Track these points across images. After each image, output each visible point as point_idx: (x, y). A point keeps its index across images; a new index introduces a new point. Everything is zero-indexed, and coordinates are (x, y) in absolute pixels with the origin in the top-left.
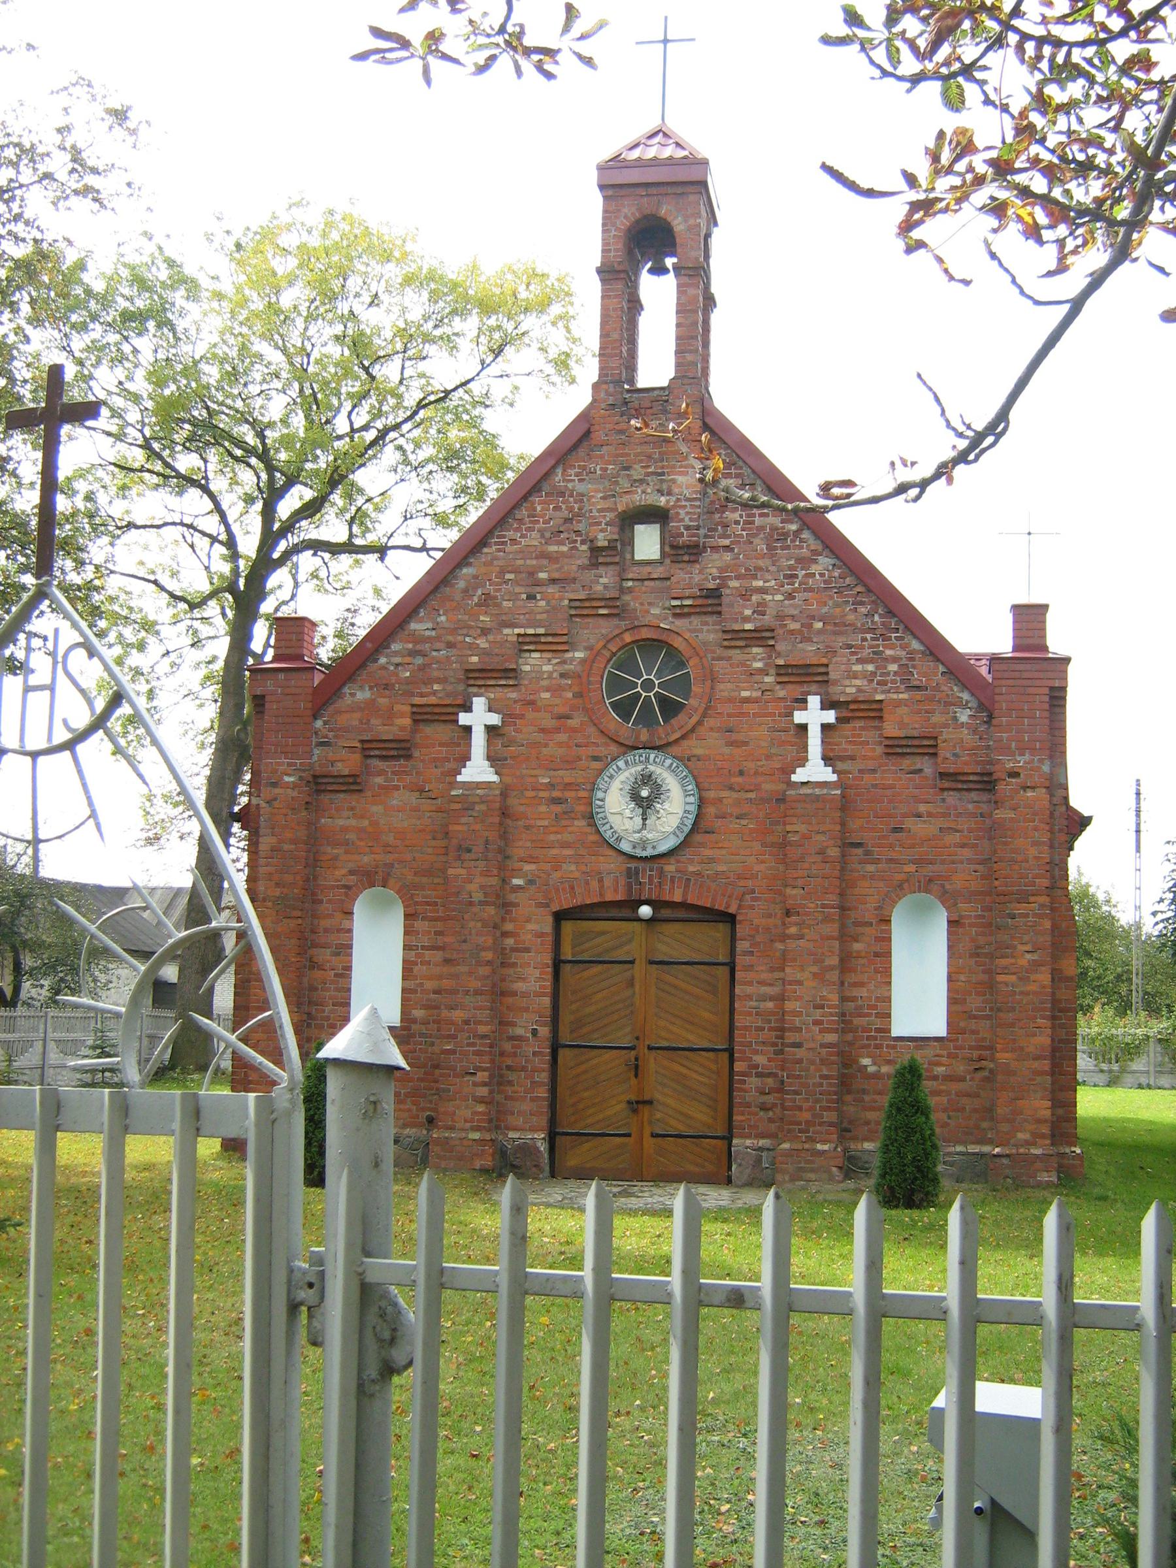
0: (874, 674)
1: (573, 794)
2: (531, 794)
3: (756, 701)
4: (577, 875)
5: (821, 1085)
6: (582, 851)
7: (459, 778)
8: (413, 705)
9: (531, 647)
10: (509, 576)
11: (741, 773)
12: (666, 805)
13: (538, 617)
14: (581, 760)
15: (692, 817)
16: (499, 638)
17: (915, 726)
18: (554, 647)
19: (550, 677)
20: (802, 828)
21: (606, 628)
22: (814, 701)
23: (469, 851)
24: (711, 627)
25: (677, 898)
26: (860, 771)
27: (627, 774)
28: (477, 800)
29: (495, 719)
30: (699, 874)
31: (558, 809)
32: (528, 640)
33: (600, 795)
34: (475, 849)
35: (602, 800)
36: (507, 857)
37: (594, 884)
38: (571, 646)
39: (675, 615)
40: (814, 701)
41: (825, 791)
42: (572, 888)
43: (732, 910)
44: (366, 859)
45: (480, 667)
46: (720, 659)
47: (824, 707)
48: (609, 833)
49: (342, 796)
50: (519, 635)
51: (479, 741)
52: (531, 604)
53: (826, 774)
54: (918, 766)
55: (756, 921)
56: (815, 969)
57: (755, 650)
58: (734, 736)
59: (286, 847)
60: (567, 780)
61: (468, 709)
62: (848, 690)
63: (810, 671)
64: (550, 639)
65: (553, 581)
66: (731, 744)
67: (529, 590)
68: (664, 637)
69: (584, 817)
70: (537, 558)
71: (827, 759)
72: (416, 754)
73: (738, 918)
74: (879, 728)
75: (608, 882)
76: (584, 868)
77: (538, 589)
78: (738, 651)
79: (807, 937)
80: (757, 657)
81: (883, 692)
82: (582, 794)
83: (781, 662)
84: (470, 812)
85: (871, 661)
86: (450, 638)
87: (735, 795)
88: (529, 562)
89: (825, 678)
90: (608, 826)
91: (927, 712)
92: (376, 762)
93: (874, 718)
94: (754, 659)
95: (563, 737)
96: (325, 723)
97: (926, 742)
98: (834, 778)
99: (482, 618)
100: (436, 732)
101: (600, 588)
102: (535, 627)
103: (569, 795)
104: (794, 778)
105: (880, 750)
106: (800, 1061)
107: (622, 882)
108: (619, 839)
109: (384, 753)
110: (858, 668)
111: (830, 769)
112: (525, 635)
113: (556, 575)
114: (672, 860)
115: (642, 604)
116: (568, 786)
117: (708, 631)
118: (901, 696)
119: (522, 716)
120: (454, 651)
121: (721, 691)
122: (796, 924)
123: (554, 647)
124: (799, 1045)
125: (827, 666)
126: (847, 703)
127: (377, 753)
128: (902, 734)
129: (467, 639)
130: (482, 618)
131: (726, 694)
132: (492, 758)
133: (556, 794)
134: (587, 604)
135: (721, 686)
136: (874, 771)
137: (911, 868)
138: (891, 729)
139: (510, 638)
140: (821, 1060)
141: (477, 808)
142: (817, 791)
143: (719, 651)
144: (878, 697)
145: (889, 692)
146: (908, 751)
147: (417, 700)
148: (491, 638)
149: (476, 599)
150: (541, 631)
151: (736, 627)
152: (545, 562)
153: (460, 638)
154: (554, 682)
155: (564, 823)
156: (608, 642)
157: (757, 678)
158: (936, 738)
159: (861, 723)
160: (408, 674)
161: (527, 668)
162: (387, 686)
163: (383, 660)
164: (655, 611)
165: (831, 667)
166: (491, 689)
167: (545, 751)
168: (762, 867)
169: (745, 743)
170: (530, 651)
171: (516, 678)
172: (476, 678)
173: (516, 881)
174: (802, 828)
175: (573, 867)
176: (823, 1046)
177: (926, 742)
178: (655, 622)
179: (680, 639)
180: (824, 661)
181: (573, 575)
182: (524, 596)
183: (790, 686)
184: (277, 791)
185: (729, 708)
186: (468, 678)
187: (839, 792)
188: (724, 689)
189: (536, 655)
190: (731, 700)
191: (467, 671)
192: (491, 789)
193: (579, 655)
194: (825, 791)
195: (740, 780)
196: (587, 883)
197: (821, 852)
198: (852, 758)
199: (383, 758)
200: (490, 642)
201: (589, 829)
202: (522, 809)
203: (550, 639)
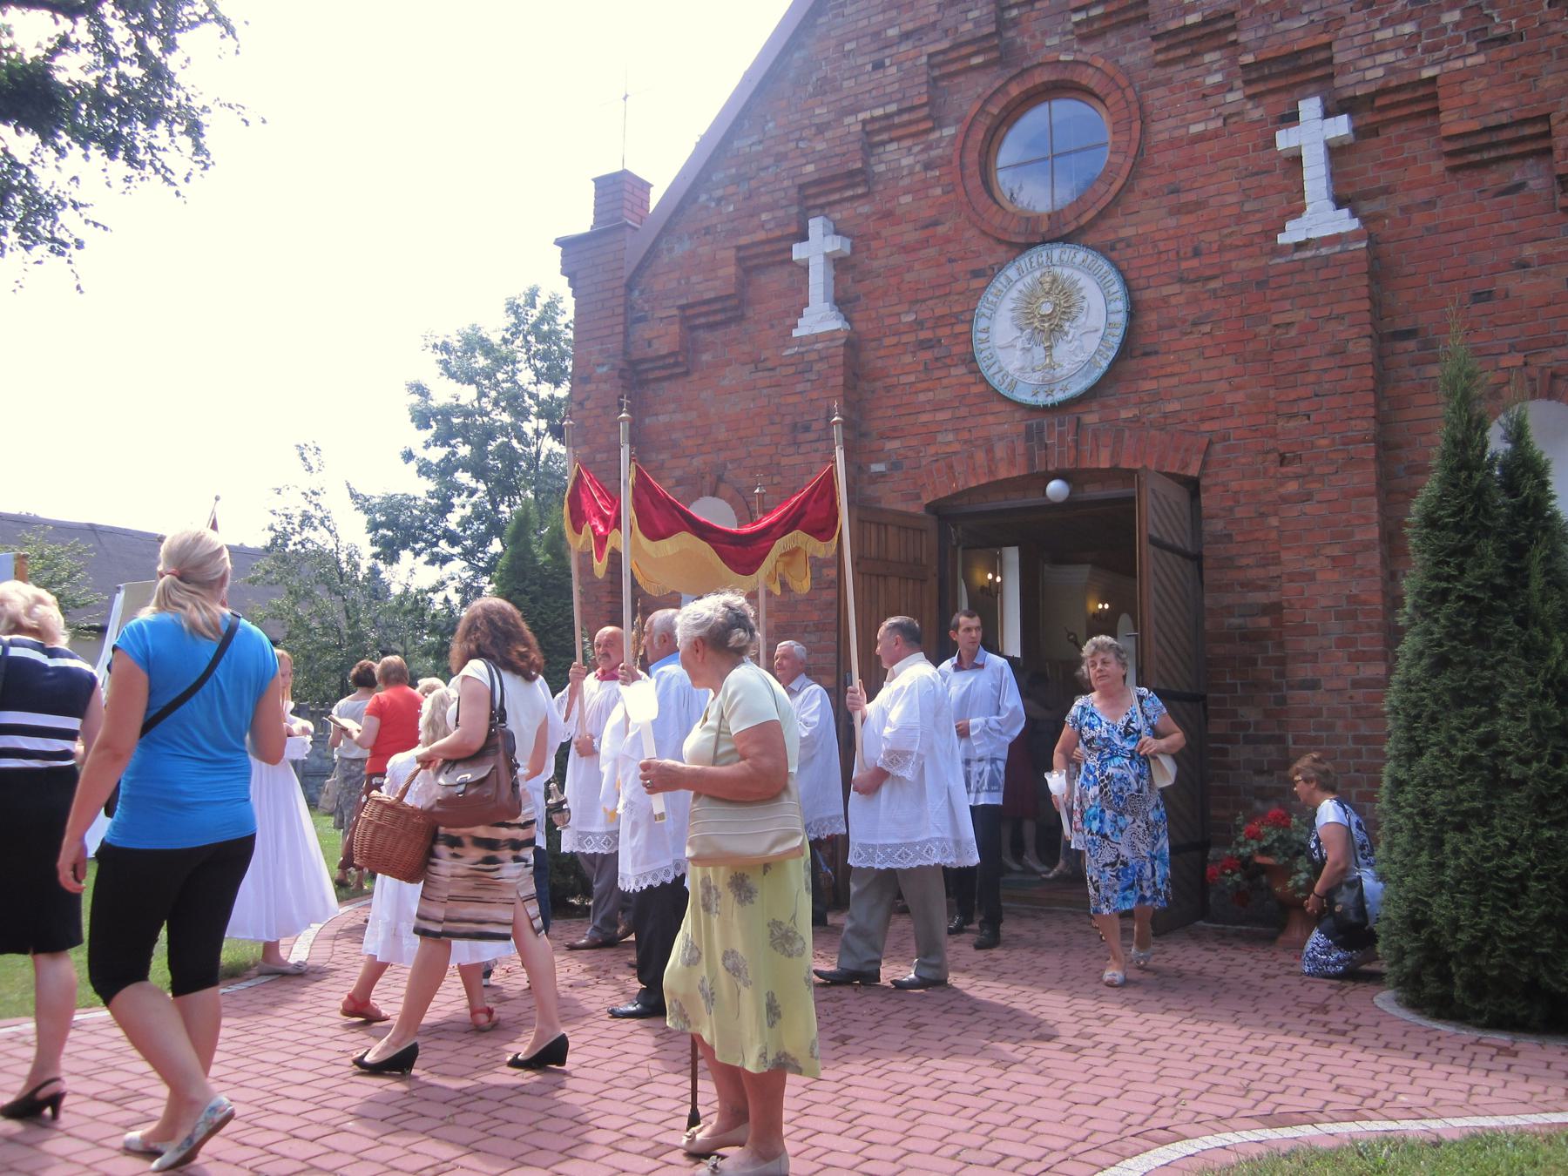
0: (1416, 36)
1: (947, 331)
2: (894, 340)
3: (1216, 135)
4: (956, 447)
5: (1358, 754)
6: (963, 411)
7: (796, 333)
8: (739, 248)
9: (885, 136)
10: (848, 47)
11: (1197, 253)
12: (1082, 319)
13: (888, 90)
14: (957, 280)
15: (1119, 332)
16: (840, 131)
17: (1503, 105)
18: (913, 129)
19: (911, 174)
20: (1299, 316)
21: (982, 84)
22: (1310, 108)
23: (807, 429)
24: (1136, 43)
25: (1104, 463)
26: (1405, 210)
27: (1020, 286)
28: (814, 356)
29: (836, 244)
30: (1136, 419)
31: (927, 355)
32: (877, 126)
33: (982, 323)
34: (815, 426)
35: (986, 331)
36: (864, 435)
37: (980, 457)
38: (939, 124)
39: (1084, 39)
40: (1310, 108)
41: (1338, 248)
42: (951, 467)
43: (1193, 471)
44: (697, 462)
45: (816, 176)
46: (1154, 85)
47: (1328, 113)
48: (998, 377)
49: (665, 384)
50: (864, 122)
51: (818, 282)
52: (878, 75)
53: (1344, 222)
54: (1517, 178)
55: (1234, 485)
56: (1336, 551)
57: (1208, 58)
58: (1185, 198)
59: (599, 457)
60: (940, 311)
61: (803, 237)
62: (1370, 75)
63: (1302, 62)
64: (906, 117)
65: (906, 36)
66: (1176, 211)
67: (876, 57)
68: (1067, 75)
69: (963, 361)
70: (884, 11)
71: (1339, 202)
72: (750, 313)
73: (1203, 482)
74: (1433, 131)
75: (1000, 451)
76: (966, 435)
77: (887, 52)
78: (1182, 66)
79: (1317, 497)
80: (1212, 68)
81: (1434, 64)
82: (960, 328)
83: (1249, 59)
84: (807, 376)
85: (1409, 18)
86: (782, 149)
87: (1188, 289)
88: (873, 20)
89: (1329, 70)
90: (994, 369)
91: (1524, 76)
92: (703, 335)
93: (1421, 115)
94: (1209, 72)
95: (932, 252)
96: (642, 293)
97: (1528, 131)
98: (1354, 224)
99: (817, 111)
100: (772, 280)
101: (969, 26)
102: (883, 105)
103: (943, 332)
104: (1282, 239)
105: (1438, 166)
106: (1317, 712)
107: (1020, 448)
108: (1013, 385)
109: (711, 319)
110: (1387, 33)
111: (1345, 212)
112: (873, 120)
113: (910, 26)
114: (1094, 406)
115: (1033, 37)
116: (940, 321)
117: (1134, 50)
118: (1470, 61)
119: (877, 236)
120: (785, 165)
121: (1160, 132)
122: (1297, 477)
123: (913, 129)
124: (1313, 685)
125: (1329, 45)
126: (1371, 97)
127: (702, 320)
128: (1475, 125)
129: (802, 145)
130: (817, 111)
131: (1166, 136)
132: (842, 302)
133: (923, 335)
134: (954, 55)
135: (1157, 126)
136: (1430, 204)
137: (1517, 359)
138: (1453, 121)
139: (853, 129)
140: (1356, 709)
141: (816, 367)
142: (1324, 251)
143: (1158, 74)
144: (1427, 73)
145: (1447, 59)
146: (1493, 154)
147: (743, 240)
148: (828, 135)
149: (810, 89)
150: (893, 108)
151: (1173, 25)
152: (894, 13)
153: (792, 145)
154: (916, 178)
155: (938, 374)
156: (986, 102)
157: (1212, 101)
158: (1546, 118)
159: (1402, 129)
160: (731, 208)
161: (881, 168)
162: (708, 231)
163: (703, 198)
164: (1054, 41)
165: (1334, 49)
166: (838, 207)
167: (908, 277)
168: (1240, 396)
169: (1199, 205)
170: (883, 143)
171: (866, 182)
172: (816, 196)
173: (877, 468)
174: (1299, 316)
175: (951, 437)
176: (1356, 684)
177: (1528, 131)
178: (1051, 56)
179: (1090, 71)
180: (1325, 38)
181: (932, 19)
182: (869, 67)
183: (1271, 99)
184: (591, 387)
185: (1171, 157)
186: (807, 198)
187: (1364, 245)
188: (1162, 130)
189: (894, 146)
190: (1173, 144)
191: (801, 187)
192: (832, 340)
193: (949, 131)
194: (1338, 248)
195: (1194, 263)
196: (971, 456)
197: (1338, 351)
198: (1387, 191)
199: (711, 326)
200: (827, 141)
201: (971, 379)
202: (879, 363)
203: (906, 117)
